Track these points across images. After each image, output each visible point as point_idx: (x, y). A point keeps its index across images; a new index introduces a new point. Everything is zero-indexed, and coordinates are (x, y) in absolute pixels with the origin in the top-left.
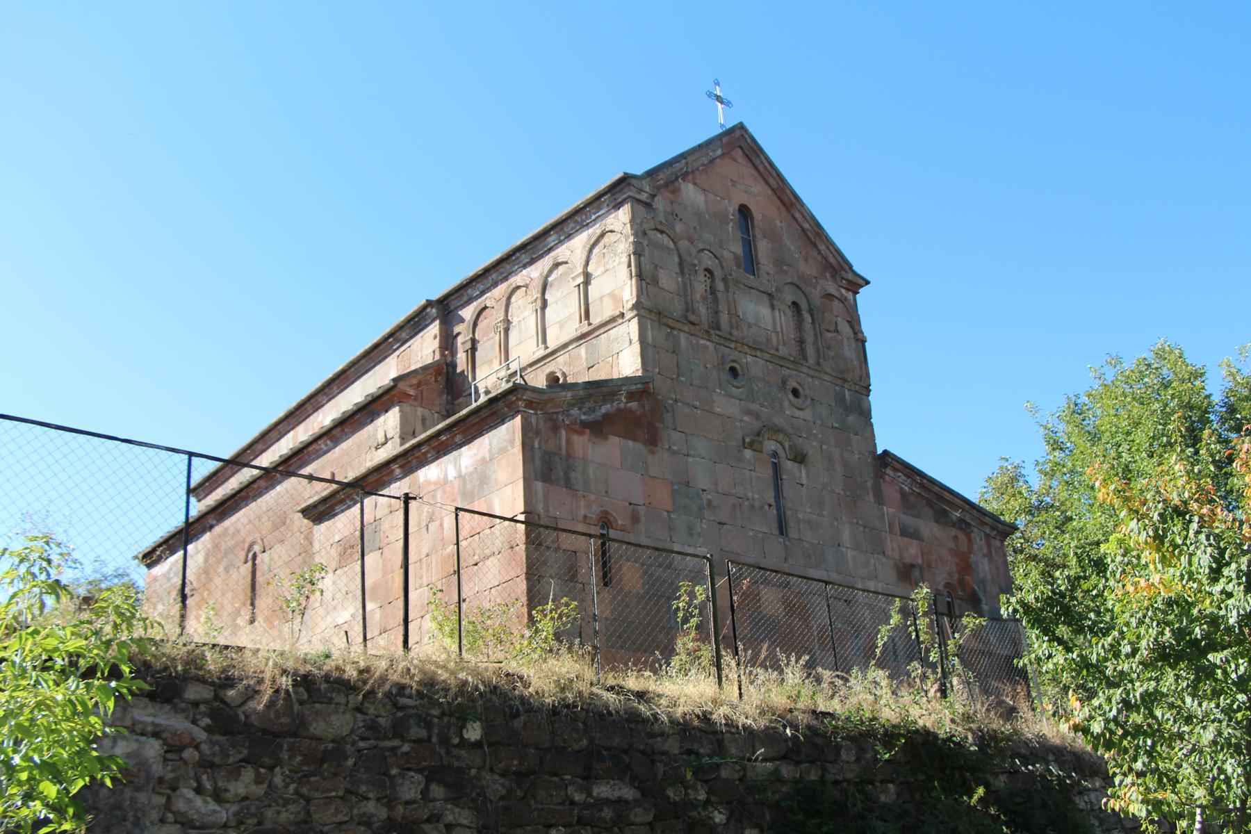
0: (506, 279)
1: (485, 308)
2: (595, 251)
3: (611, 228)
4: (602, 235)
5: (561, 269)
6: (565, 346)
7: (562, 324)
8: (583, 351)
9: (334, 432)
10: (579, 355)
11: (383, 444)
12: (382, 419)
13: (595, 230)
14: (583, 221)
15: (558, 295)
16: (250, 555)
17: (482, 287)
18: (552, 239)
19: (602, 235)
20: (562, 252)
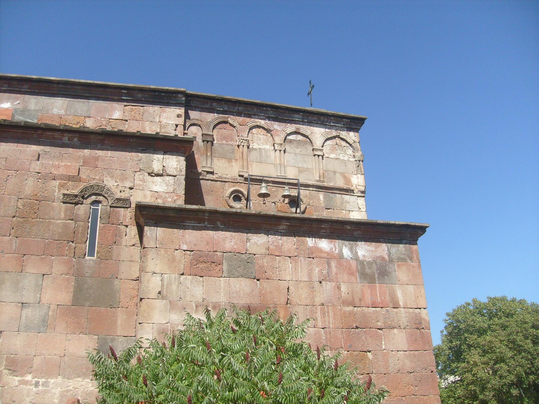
0: (250, 116)
1: (226, 122)
2: (328, 142)
3: (345, 138)
4: (335, 137)
5: (300, 137)
7: (301, 171)
8: (321, 196)
9: (92, 137)
10: (319, 197)
11: (158, 175)
12: (160, 157)
13: (334, 133)
14: (323, 121)
15: (298, 151)
17: (226, 108)
18: (297, 117)
19: (335, 137)
20: (305, 129)
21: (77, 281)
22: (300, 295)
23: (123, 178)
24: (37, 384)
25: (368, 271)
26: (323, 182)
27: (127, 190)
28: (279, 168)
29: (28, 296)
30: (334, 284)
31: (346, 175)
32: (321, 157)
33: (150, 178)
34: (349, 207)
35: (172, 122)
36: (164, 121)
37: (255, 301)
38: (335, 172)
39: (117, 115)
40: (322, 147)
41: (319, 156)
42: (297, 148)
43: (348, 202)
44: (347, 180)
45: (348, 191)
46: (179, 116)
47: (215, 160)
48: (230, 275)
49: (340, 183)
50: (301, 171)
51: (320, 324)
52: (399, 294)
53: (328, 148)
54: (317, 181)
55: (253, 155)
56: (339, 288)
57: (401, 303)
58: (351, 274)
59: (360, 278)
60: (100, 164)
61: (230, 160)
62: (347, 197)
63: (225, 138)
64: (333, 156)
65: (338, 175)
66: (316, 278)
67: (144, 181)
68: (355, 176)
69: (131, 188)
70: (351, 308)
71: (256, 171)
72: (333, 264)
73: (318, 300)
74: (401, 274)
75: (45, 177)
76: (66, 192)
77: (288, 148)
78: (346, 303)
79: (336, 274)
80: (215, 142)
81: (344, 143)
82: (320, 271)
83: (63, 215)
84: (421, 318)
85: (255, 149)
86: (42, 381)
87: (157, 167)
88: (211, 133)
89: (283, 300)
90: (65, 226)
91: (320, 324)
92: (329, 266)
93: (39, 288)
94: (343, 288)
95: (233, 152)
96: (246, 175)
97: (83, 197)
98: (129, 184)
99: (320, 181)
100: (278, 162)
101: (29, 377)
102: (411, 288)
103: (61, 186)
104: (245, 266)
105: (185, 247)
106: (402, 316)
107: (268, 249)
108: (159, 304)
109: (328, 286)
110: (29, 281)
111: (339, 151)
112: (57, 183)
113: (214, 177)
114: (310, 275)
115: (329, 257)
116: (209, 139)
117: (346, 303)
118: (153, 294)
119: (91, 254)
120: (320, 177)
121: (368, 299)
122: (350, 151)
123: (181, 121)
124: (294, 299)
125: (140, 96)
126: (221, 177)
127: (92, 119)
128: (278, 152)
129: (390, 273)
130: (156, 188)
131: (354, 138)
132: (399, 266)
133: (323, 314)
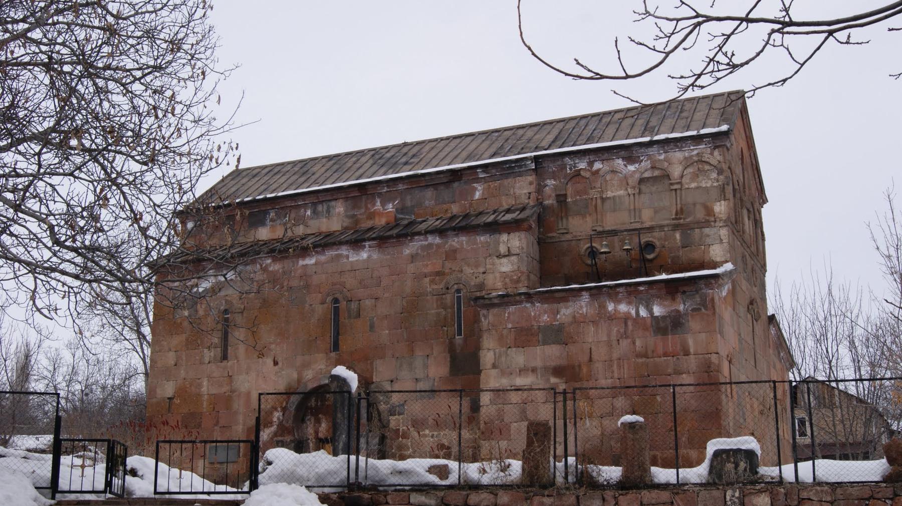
2: (690, 170)
6: (661, 227)
11: (505, 256)
14: (682, 147)
15: (654, 189)
16: (329, 299)
21: (451, 357)
22: (600, 353)
23: (477, 266)
24: (432, 436)
25: (662, 325)
26: (680, 219)
27: (481, 275)
28: (633, 213)
29: (420, 374)
30: (629, 340)
31: (709, 204)
32: (678, 192)
33: (497, 261)
34: (708, 241)
35: (525, 191)
36: (518, 192)
37: (563, 362)
38: (694, 204)
39: (477, 195)
40: (682, 177)
41: (676, 190)
42: (653, 186)
43: (708, 236)
44: (709, 211)
45: (707, 224)
46: (531, 183)
47: (570, 219)
48: (545, 343)
49: (700, 214)
50: (656, 212)
51: (616, 375)
52: (691, 342)
53: (689, 176)
54: (673, 219)
55: (608, 204)
56: (634, 343)
57: (692, 351)
58: (646, 329)
59: (654, 332)
60: (458, 256)
61: (584, 216)
62: (707, 231)
63: (578, 193)
64: (693, 185)
65: (698, 207)
66: (614, 338)
67: (493, 264)
68: (718, 204)
69: (484, 273)
70: (644, 359)
71: (610, 222)
72: (630, 323)
73: (615, 356)
74: (694, 324)
75: (419, 277)
76: (436, 287)
77: (643, 187)
78: (639, 355)
79: (632, 331)
80: (569, 200)
81: (707, 167)
82: (618, 331)
83: (435, 305)
84: (710, 363)
85: (609, 198)
86: (435, 433)
87: (503, 249)
88: (562, 193)
89: (586, 358)
90: (438, 314)
91: (616, 375)
92: (626, 324)
93: (426, 366)
94: (638, 343)
95: (587, 207)
96: (599, 229)
97: (448, 288)
98: (482, 270)
99: (676, 219)
100: (632, 207)
101: (427, 432)
102: (703, 336)
103: (432, 282)
104: (557, 335)
105: (510, 326)
106: (692, 362)
107: (574, 317)
108: (494, 372)
109: (625, 343)
110: (418, 362)
111: (701, 178)
112: (427, 280)
113: (568, 237)
114: (609, 335)
115: (626, 318)
116: (562, 199)
117: (639, 355)
118: (489, 366)
119: (460, 334)
120: (676, 214)
121: (660, 351)
122: (714, 175)
123: (532, 188)
124: (595, 356)
125: (494, 171)
126: (575, 236)
127: (457, 204)
128: (632, 196)
129: (683, 324)
130: (504, 269)
131: (719, 158)
132: (692, 316)
133: (619, 367)
